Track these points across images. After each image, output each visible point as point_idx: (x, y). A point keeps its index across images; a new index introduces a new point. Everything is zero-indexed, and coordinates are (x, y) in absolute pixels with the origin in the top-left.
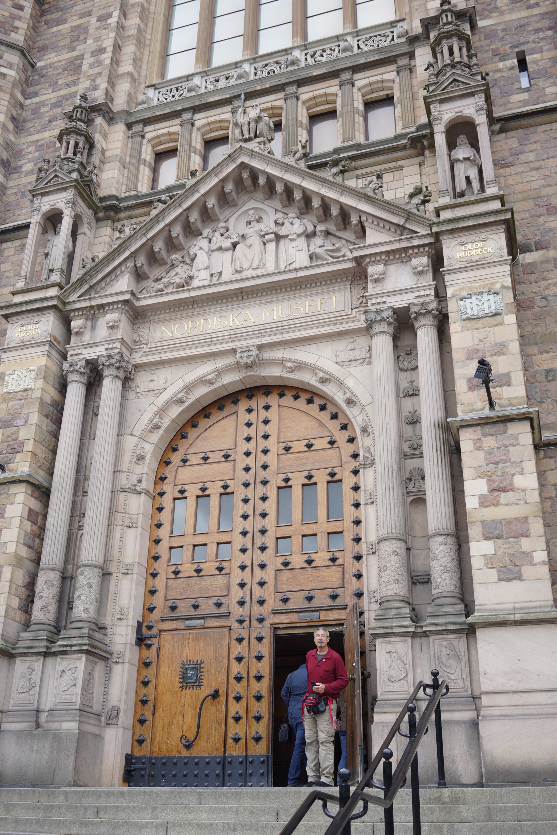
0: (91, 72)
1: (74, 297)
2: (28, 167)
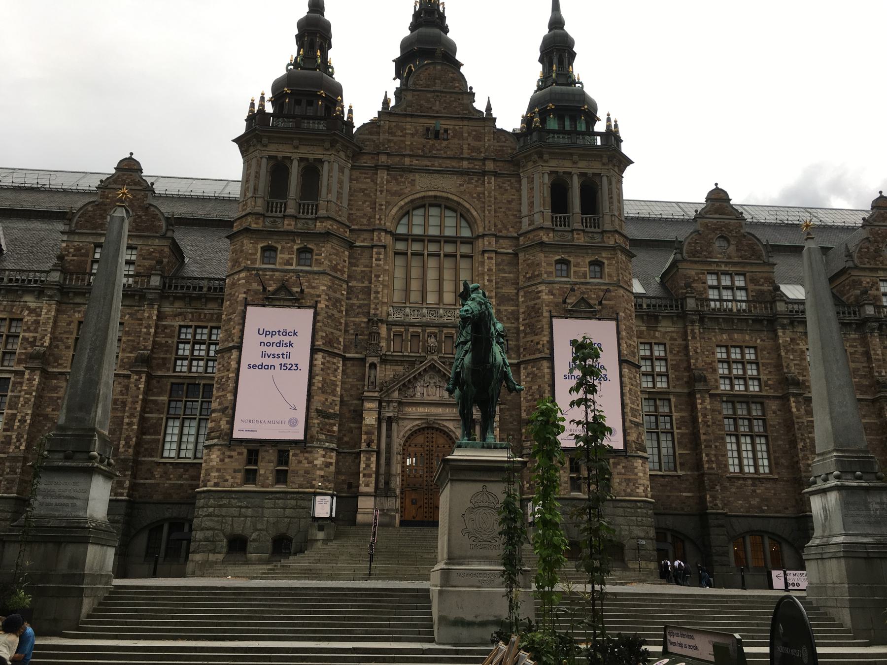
0: (375, 301)
1: (383, 396)
2: (351, 332)
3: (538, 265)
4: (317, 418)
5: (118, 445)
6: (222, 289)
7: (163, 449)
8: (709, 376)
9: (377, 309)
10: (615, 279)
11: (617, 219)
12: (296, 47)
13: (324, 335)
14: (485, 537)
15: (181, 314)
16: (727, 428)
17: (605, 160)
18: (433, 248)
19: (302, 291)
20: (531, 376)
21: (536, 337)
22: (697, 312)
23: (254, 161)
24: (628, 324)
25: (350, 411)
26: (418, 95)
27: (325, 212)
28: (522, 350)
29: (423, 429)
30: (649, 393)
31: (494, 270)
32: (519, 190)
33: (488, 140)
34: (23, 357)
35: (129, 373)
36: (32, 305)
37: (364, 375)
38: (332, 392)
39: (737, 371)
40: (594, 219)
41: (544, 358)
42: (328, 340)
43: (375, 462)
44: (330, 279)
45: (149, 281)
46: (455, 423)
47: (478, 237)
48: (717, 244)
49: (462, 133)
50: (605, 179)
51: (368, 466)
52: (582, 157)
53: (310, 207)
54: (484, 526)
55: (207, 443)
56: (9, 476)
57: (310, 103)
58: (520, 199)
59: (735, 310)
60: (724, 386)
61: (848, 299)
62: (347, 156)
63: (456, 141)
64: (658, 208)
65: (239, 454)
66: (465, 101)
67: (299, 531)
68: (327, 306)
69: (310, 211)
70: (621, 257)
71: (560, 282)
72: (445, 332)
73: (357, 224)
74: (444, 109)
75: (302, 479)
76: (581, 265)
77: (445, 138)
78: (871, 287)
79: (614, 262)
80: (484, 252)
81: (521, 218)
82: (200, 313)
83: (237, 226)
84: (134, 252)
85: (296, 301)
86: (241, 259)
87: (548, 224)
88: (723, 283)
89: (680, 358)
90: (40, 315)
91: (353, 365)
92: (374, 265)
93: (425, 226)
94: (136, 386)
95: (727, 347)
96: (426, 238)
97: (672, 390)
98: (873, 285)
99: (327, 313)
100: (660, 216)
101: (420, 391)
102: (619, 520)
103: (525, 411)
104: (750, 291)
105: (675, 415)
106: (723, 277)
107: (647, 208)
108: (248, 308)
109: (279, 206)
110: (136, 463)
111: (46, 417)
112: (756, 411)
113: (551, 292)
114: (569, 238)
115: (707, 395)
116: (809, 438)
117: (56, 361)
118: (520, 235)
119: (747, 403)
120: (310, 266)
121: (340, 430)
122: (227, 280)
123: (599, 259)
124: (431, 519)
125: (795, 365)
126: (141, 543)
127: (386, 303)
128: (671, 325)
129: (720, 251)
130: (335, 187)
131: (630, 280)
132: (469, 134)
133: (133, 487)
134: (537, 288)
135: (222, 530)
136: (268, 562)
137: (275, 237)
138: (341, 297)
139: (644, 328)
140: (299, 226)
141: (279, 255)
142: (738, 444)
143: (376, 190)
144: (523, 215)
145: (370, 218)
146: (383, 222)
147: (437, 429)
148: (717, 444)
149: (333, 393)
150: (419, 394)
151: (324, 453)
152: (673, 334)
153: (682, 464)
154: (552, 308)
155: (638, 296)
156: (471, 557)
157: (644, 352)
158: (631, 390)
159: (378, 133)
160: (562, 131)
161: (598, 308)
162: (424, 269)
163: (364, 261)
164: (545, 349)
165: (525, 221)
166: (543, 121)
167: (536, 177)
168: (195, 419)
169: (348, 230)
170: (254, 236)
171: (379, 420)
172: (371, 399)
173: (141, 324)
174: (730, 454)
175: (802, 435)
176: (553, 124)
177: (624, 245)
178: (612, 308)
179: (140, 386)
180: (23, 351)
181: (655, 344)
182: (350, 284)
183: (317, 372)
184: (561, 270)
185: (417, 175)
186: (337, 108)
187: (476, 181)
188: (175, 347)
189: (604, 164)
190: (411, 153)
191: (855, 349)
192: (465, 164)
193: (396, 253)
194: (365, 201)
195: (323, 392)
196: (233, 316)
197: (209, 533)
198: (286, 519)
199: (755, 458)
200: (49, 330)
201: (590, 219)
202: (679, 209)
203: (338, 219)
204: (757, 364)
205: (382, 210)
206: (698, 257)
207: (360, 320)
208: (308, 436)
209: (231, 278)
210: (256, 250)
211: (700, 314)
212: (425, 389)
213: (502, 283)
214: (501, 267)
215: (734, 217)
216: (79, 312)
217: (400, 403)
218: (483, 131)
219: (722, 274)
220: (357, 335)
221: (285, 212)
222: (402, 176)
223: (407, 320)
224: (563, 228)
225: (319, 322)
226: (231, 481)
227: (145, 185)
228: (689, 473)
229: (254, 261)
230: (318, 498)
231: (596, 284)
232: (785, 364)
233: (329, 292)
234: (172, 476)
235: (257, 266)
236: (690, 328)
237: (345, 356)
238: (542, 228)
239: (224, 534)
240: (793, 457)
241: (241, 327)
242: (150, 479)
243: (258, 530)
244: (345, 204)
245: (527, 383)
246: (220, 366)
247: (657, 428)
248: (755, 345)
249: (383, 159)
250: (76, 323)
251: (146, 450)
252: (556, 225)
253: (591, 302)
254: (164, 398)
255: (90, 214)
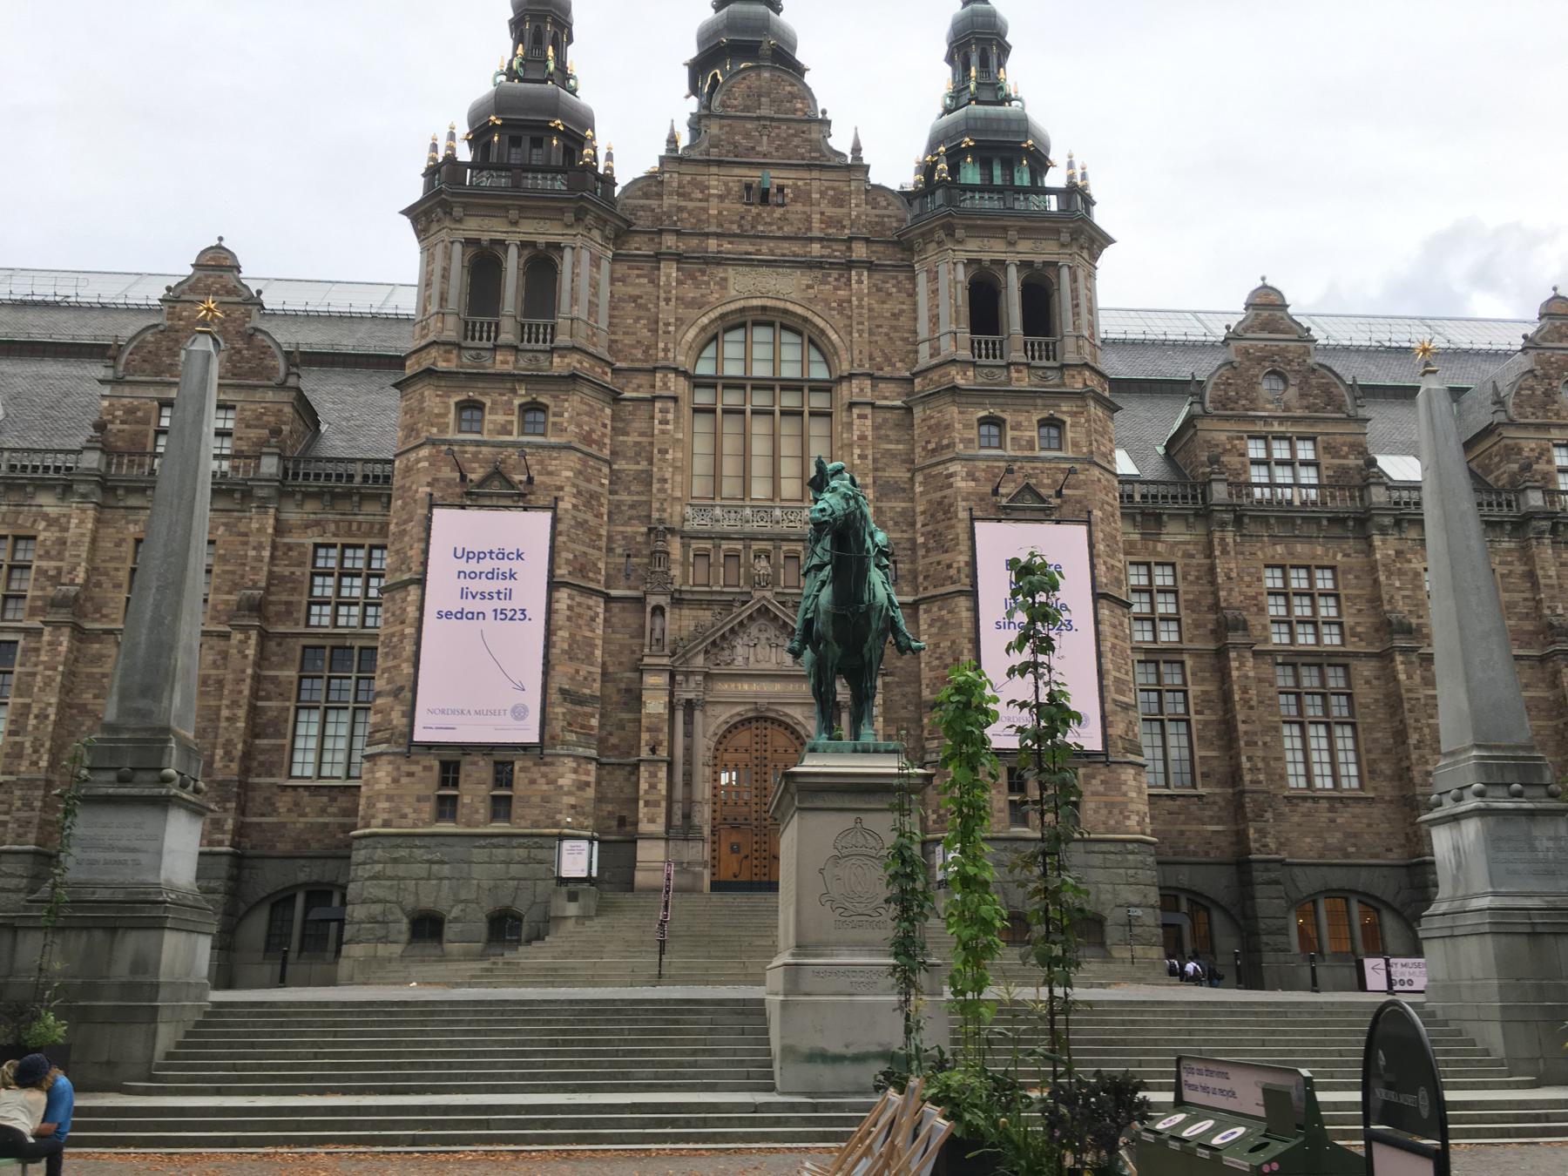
1: (677, 664)
2: (619, 551)
3: (947, 427)
4: (561, 705)
5: (212, 756)
6: (387, 479)
7: (291, 762)
8: (1252, 620)
9: (664, 510)
10: (1085, 450)
11: (1087, 343)
12: (510, 43)
13: (571, 556)
14: (861, 908)
15: (317, 523)
16: (1284, 711)
17: (1065, 237)
18: (760, 399)
19: (530, 480)
20: (938, 624)
21: (947, 556)
22: (1230, 508)
23: (440, 247)
24: (1108, 529)
25: (619, 691)
26: (729, 125)
27: (567, 338)
28: (921, 578)
29: (749, 720)
30: (1147, 651)
31: (870, 438)
32: (912, 295)
33: (856, 206)
34: (39, 603)
35: (228, 629)
36: (52, 511)
37: (643, 627)
38: (588, 657)
39: (1302, 609)
40: (1047, 345)
41: (960, 593)
42: (578, 566)
43: (665, 781)
44: (579, 459)
45: (258, 466)
46: (805, 708)
47: (841, 379)
48: (1265, 385)
49: (809, 193)
50: (1065, 272)
51: (653, 786)
52: (1024, 232)
53: (541, 330)
54: (859, 888)
55: (369, 751)
56: (23, 814)
57: (537, 143)
58: (915, 311)
59: (1297, 502)
60: (1279, 638)
61: (1497, 479)
62: (606, 238)
63: (799, 207)
64: (1160, 323)
65: (426, 768)
66: (814, 136)
67: (534, 903)
68: (575, 506)
69: (541, 337)
70: (1095, 411)
71: (987, 458)
72: (784, 548)
73: (625, 360)
74: (777, 150)
75: (537, 812)
76: (1025, 426)
77: (780, 201)
78: (1538, 458)
79: (1083, 420)
80: (852, 405)
81: (916, 343)
82: (350, 523)
83: (412, 365)
84: (231, 414)
85: (520, 497)
86: (420, 425)
87: (965, 354)
88: (1277, 455)
89: (1200, 588)
90: (67, 530)
91: (624, 610)
92: (656, 432)
93: (747, 360)
94: (241, 652)
95: (1282, 567)
96: (749, 383)
97: (1186, 645)
98: (1541, 454)
99: (574, 518)
100: (1163, 337)
101: (742, 654)
102: (1097, 875)
103: (927, 686)
104: (1323, 467)
105: (1193, 690)
106: (1275, 444)
107: (1140, 322)
108: (436, 511)
109: (485, 328)
110: (243, 785)
111: (83, 709)
112: (1335, 680)
113: (971, 476)
114: (1003, 378)
115: (1249, 654)
116: (1429, 726)
117: (98, 609)
118: (915, 375)
119: (1320, 666)
120: (543, 435)
121: (602, 726)
122: (397, 463)
123: (1057, 415)
124: (766, 879)
125: (1404, 597)
126: (257, 925)
127: (679, 499)
128: (1183, 530)
129: (1271, 398)
130: (584, 294)
131: (1112, 451)
132: (823, 194)
133: (240, 830)
134: (947, 469)
135: (399, 903)
136: (482, 956)
137: (480, 385)
138: (599, 489)
139: (1137, 537)
140: (522, 364)
141: (488, 417)
142: (1304, 737)
143: (658, 298)
144: (920, 338)
145: (648, 347)
146: (671, 355)
147: (773, 720)
148: (1268, 739)
149: (589, 659)
150: (740, 659)
151: (574, 765)
152: (1188, 547)
153: (1205, 775)
154: (972, 504)
155: (1126, 480)
156: (838, 944)
157: (1138, 578)
158: (1114, 647)
159: (660, 196)
160: (987, 188)
161: (1055, 502)
162: (745, 436)
163: (638, 425)
164: (963, 576)
165: (924, 349)
166: (954, 169)
167: (943, 269)
168: (347, 708)
169: (609, 370)
170: (443, 384)
171: (672, 707)
172: (656, 669)
173: (246, 543)
174: (1289, 756)
175: (1417, 721)
176: (971, 174)
177: (1099, 390)
178: (1080, 502)
179: (247, 652)
180: (39, 593)
181: (1157, 564)
182: (615, 467)
183: (560, 623)
184: (989, 436)
185: (730, 269)
186: (585, 152)
187: (836, 280)
188: (307, 585)
189: (1063, 245)
190: (719, 230)
191: (1510, 568)
192: (816, 248)
193: (696, 411)
194: (637, 319)
195: (571, 659)
196: (409, 527)
197: (377, 909)
198: (511, 882)
199: (1333, 763)
200: (84, 555)
201: (1040, 344)
202: (1197, 324)
203: (591, 350)
204: (1337, 597)
205: (669, 333)
206: (1232, 409)
207: (635, 529)
208: (547, 737)
209: (404, 458)
210: (447, 407)
211: (1235, 511)
212: (752, 650)
213: (884, 460)
214: (883, 432)
215: (1295, 337)
216: (136, 522)
217: (708, 676)
218: (846, 189)
219: (1274, 438)
220: (628, 556)
221: (496, 339)
222: (703, 273)
223: (717, 528)
224: (991, 361)
225: (560, 534)
226: (412, 816)
227: (247, 294)
228: (1218, 790)
229: (443, 428)
230: (566, 845)
231: (1050, 460)
232: (1385, 597)
233: (577, 481)
234: (308, 810)
235: (449, 436)
236: (1217, 535)
237: (607, 594)
238: (953, 362)
239: (403, 910)
240: (1401, 760)
241: (422, 545)
242: (270, 815)
243: (462, 901)
244: (603, 324)
245: (930, 636)
246: (389, 615)
247: (1162, 714)
248: (1333, 563)
249: (669, 241)
250: (131, 543)
251: (262, 764)
252: (980, 357)
253: (1043, 491)
254: (291, 673)
255: (151, 347)
